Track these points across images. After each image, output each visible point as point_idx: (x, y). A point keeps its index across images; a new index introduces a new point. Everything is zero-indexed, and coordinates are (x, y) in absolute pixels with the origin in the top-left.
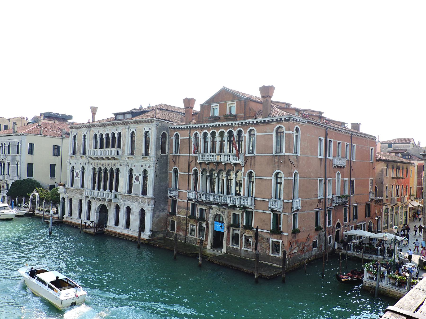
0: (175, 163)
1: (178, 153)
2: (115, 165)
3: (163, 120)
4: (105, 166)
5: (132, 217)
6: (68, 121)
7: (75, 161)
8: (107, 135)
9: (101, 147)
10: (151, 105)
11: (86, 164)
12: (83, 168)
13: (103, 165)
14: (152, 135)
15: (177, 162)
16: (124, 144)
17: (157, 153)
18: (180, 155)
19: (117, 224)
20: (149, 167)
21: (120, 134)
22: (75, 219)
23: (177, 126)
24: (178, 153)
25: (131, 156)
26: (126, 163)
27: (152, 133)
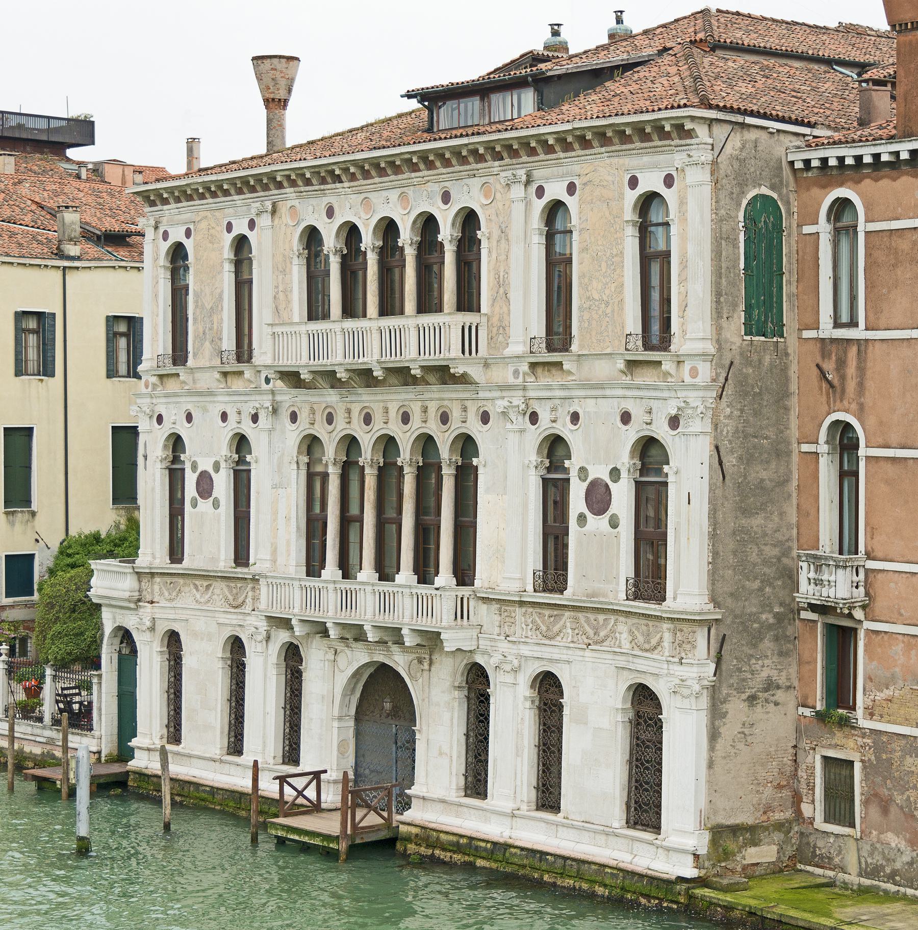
0: (834, 390)
1: (853, 323)
2: (444, 418)
3: (752, 114)
4: (379, 427)
6: (71, 153)
7: (188, 404)
8: (389, 228)
9: (351, 309)
10: (635, 24)
11: (255, 418)
12: (241, 443)
13: (368, 419)
14: (683, 218)
15: (851, 386)
16: (501, 283)
17: (719, 329)
18: (871, 335)
19: (476, 783)
20: (674, 422)
21: (469, 220)
22: (202, 760)
23: (841, 152)
24: (853, 324)
25: (555, 357)
26: (518, 401)
27: (682, 202)
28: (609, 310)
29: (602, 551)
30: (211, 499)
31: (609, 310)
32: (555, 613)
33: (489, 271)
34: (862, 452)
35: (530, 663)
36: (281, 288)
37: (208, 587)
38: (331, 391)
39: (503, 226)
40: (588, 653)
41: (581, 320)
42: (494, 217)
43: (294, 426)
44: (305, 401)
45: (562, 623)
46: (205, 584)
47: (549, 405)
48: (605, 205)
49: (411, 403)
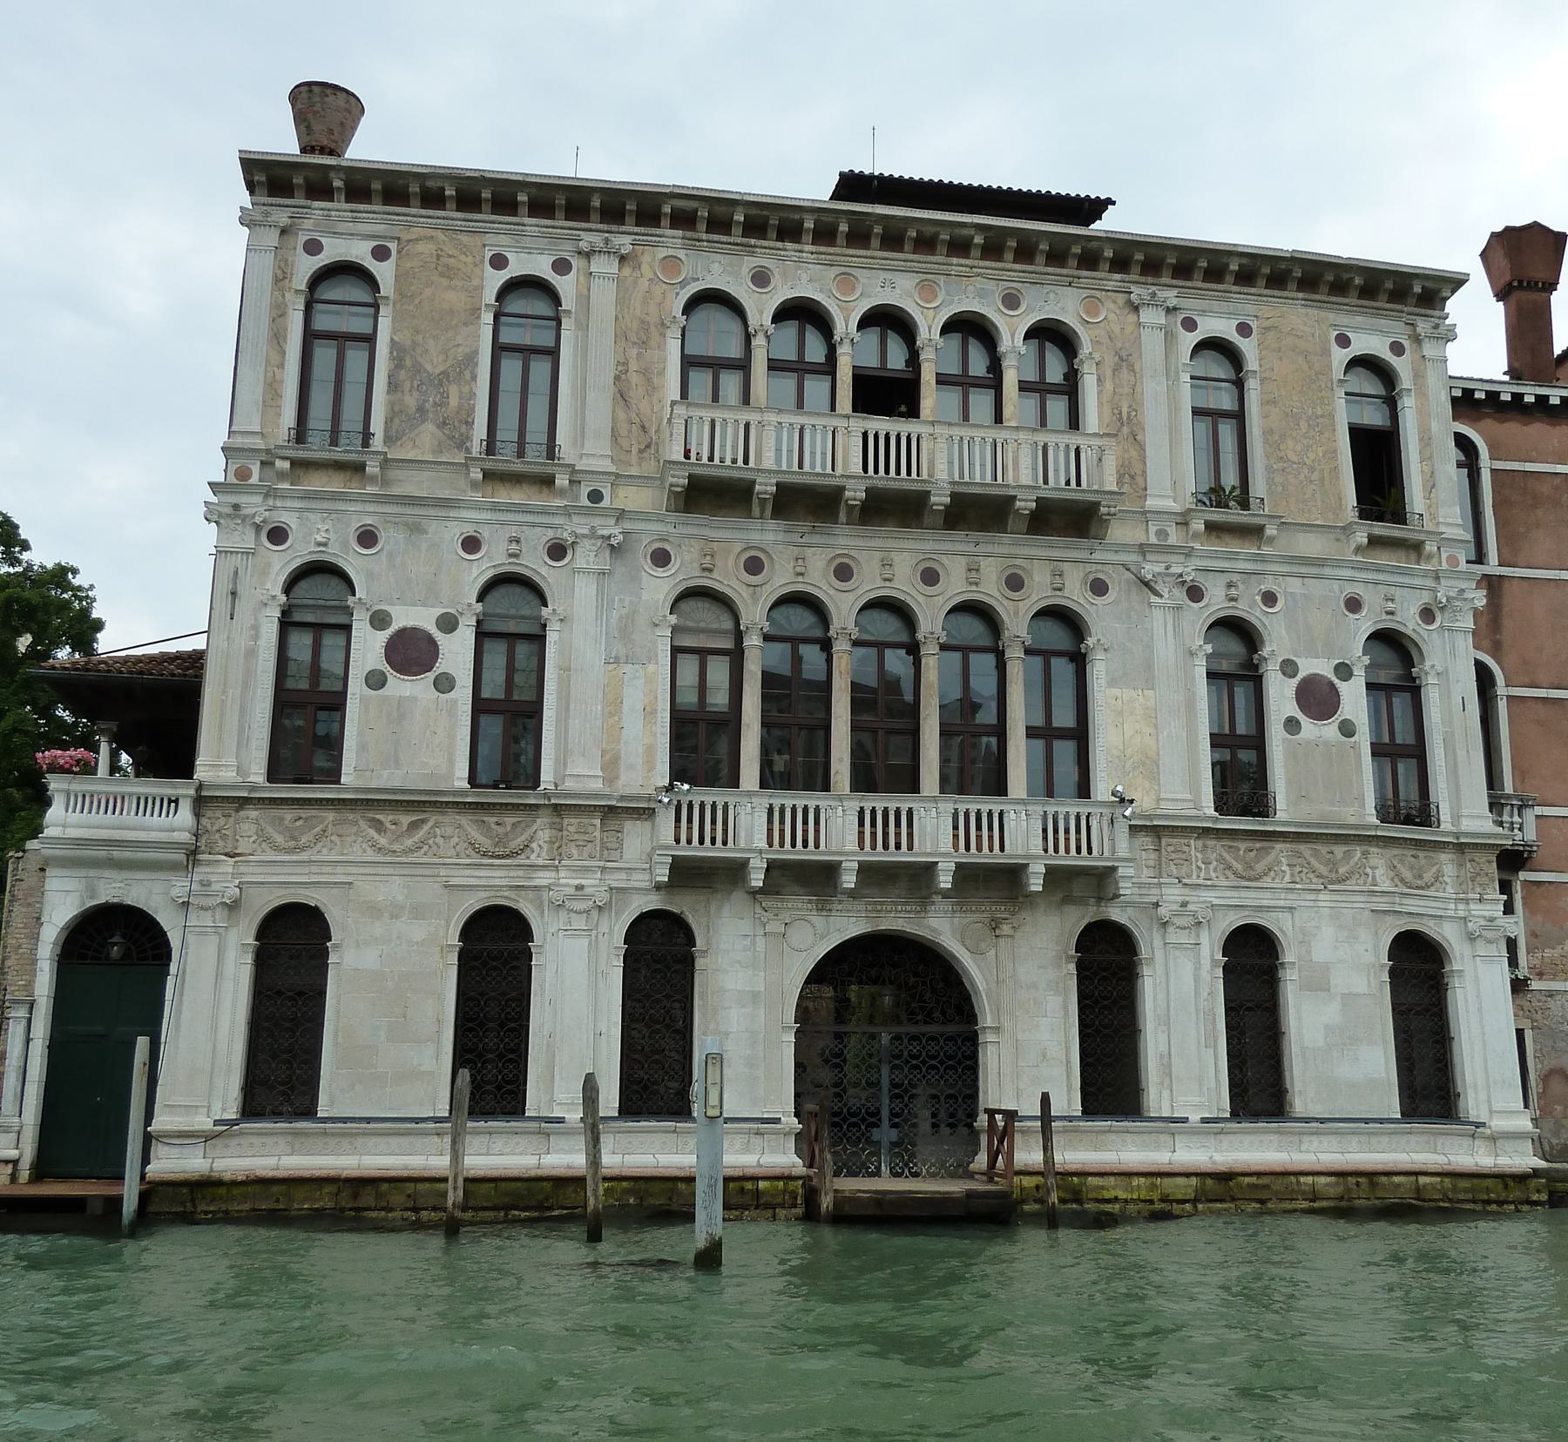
5: (1306, 1020)
7: (362, 515)
18: (1505, 571)
27: (1418, 375)
28: (1315, 476)
29: (1322, 768)
30: (431, 676)
31: (1315, 476)
32: (1258, 845)
33: (1100, 404)
34: (1501, 689)
35: (1220, 914)
36: (633, 366)
37: (414, 826)
38: (772, 524)
39: (1124, 354)
40: (1321, 897)
41: (1270, 482)
42: (1105, 340)
43: (660, 572)
44: (691, 537)
45: (1270, 858)
46: (405, 820)
47: (1222, 580)
48: (1301, 360)
49: (944, 559)
